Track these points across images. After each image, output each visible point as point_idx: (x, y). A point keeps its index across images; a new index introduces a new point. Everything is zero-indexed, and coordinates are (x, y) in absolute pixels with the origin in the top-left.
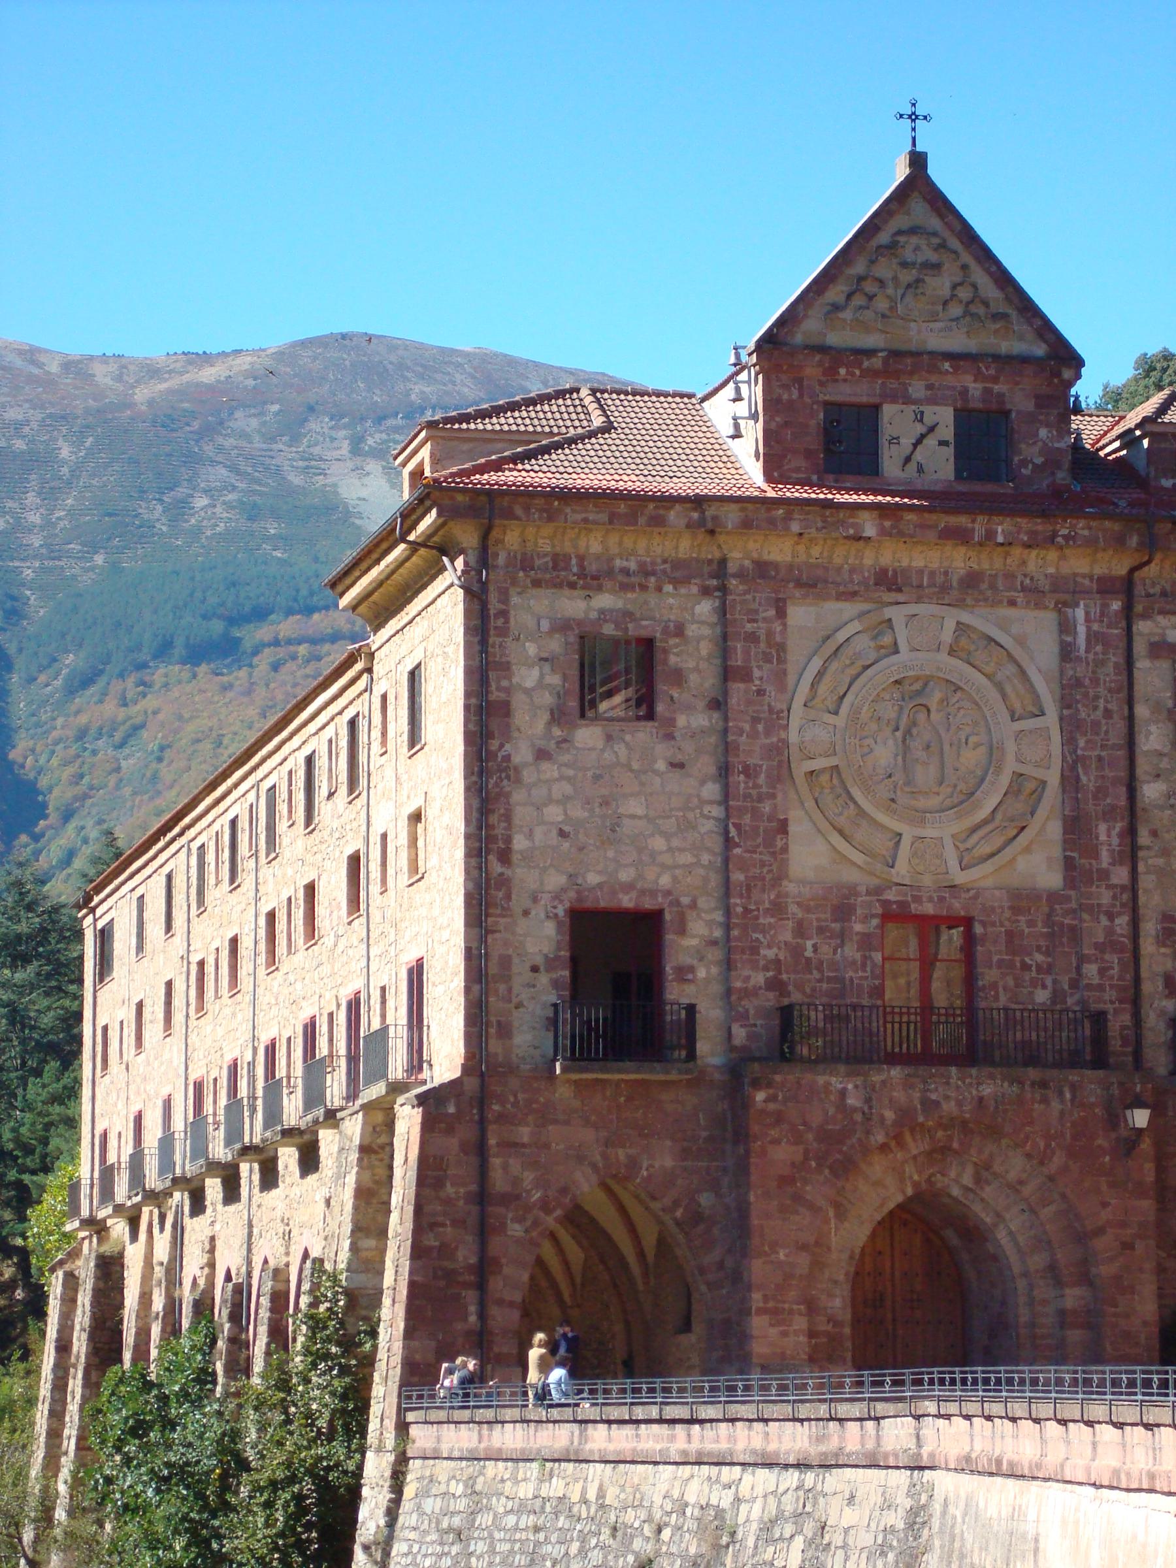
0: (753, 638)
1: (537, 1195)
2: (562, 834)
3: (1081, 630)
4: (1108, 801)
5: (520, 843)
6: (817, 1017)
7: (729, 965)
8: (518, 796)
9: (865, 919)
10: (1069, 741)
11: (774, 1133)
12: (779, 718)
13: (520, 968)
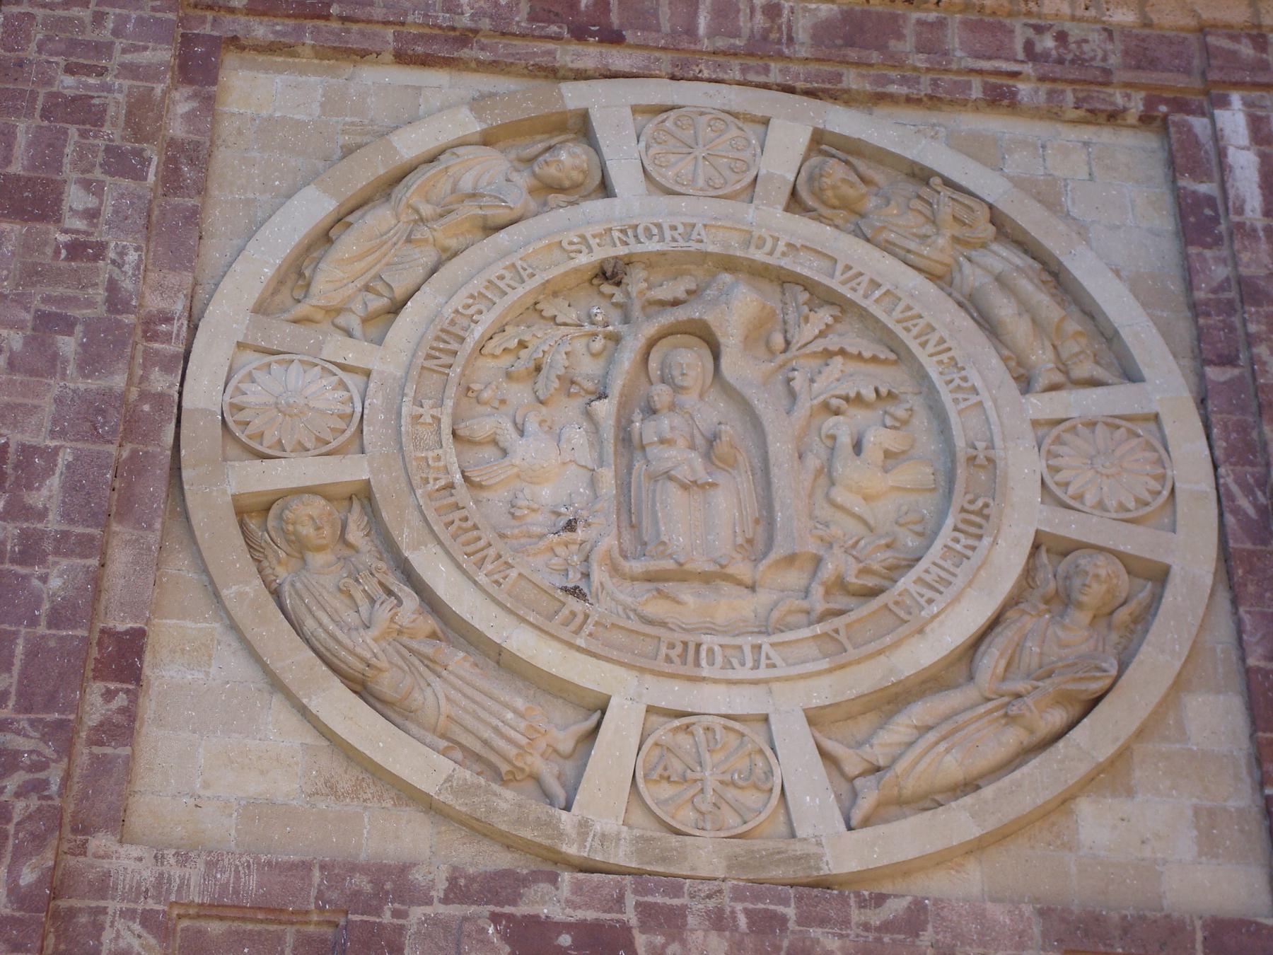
3: (1245, 165)
12: (150, 334)
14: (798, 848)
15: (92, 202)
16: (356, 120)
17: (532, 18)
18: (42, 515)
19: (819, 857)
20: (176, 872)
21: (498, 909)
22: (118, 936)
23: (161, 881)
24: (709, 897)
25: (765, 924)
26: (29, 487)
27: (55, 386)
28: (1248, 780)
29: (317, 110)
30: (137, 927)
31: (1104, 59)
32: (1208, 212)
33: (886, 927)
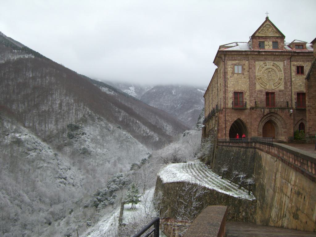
0: (252, 65)
1: (231, 120)
2: (233, 85)
3: (286, 63)
5: (229, 86)
6: (259, 103)
7: (250, 97)
8: (228, 81)
9: (264, 93)
10: (285, 74)
11: (254, 114)
13: (229, 98)
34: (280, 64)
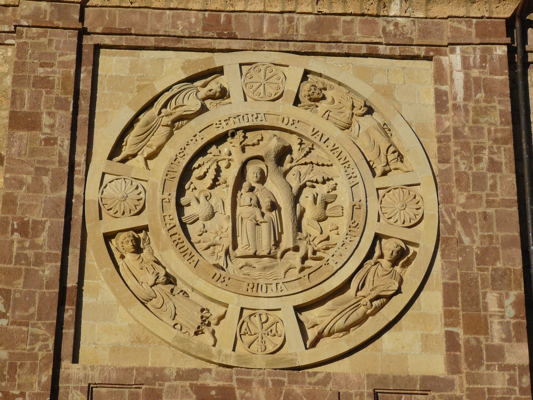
0: (45, 83)
3: (459, 77)
4: (499, 265)
10: (445, 198)
14: (290, 357)
15: (52, 121)
16: (141, 75)
17: (204, 29)
18: (41, 247)
19: (295, 360)
20: (90, 373)
21: (192, 382)
22: (73, 396)
23: (86, 376)
24: (260, 375)
25: (279, 384)
26: (37, 236)
27: (43, 196)
28: (440, 323)
29: (128, 72)
30: (79, 392)
31: (411, 34)
32: (444, 98)
33: (317, 383)
34: (387, 91)
